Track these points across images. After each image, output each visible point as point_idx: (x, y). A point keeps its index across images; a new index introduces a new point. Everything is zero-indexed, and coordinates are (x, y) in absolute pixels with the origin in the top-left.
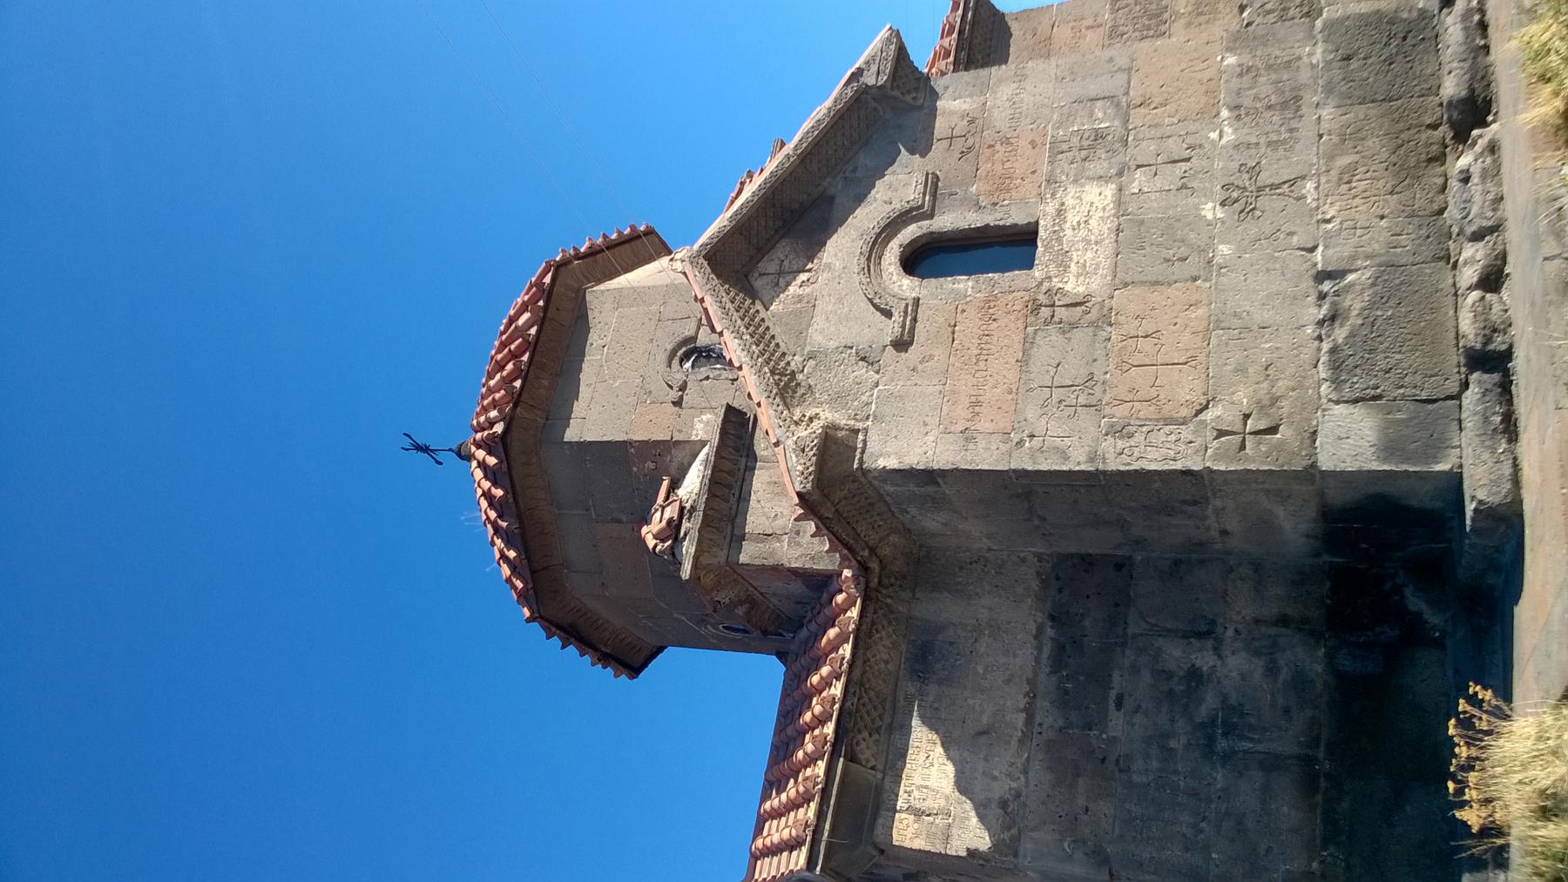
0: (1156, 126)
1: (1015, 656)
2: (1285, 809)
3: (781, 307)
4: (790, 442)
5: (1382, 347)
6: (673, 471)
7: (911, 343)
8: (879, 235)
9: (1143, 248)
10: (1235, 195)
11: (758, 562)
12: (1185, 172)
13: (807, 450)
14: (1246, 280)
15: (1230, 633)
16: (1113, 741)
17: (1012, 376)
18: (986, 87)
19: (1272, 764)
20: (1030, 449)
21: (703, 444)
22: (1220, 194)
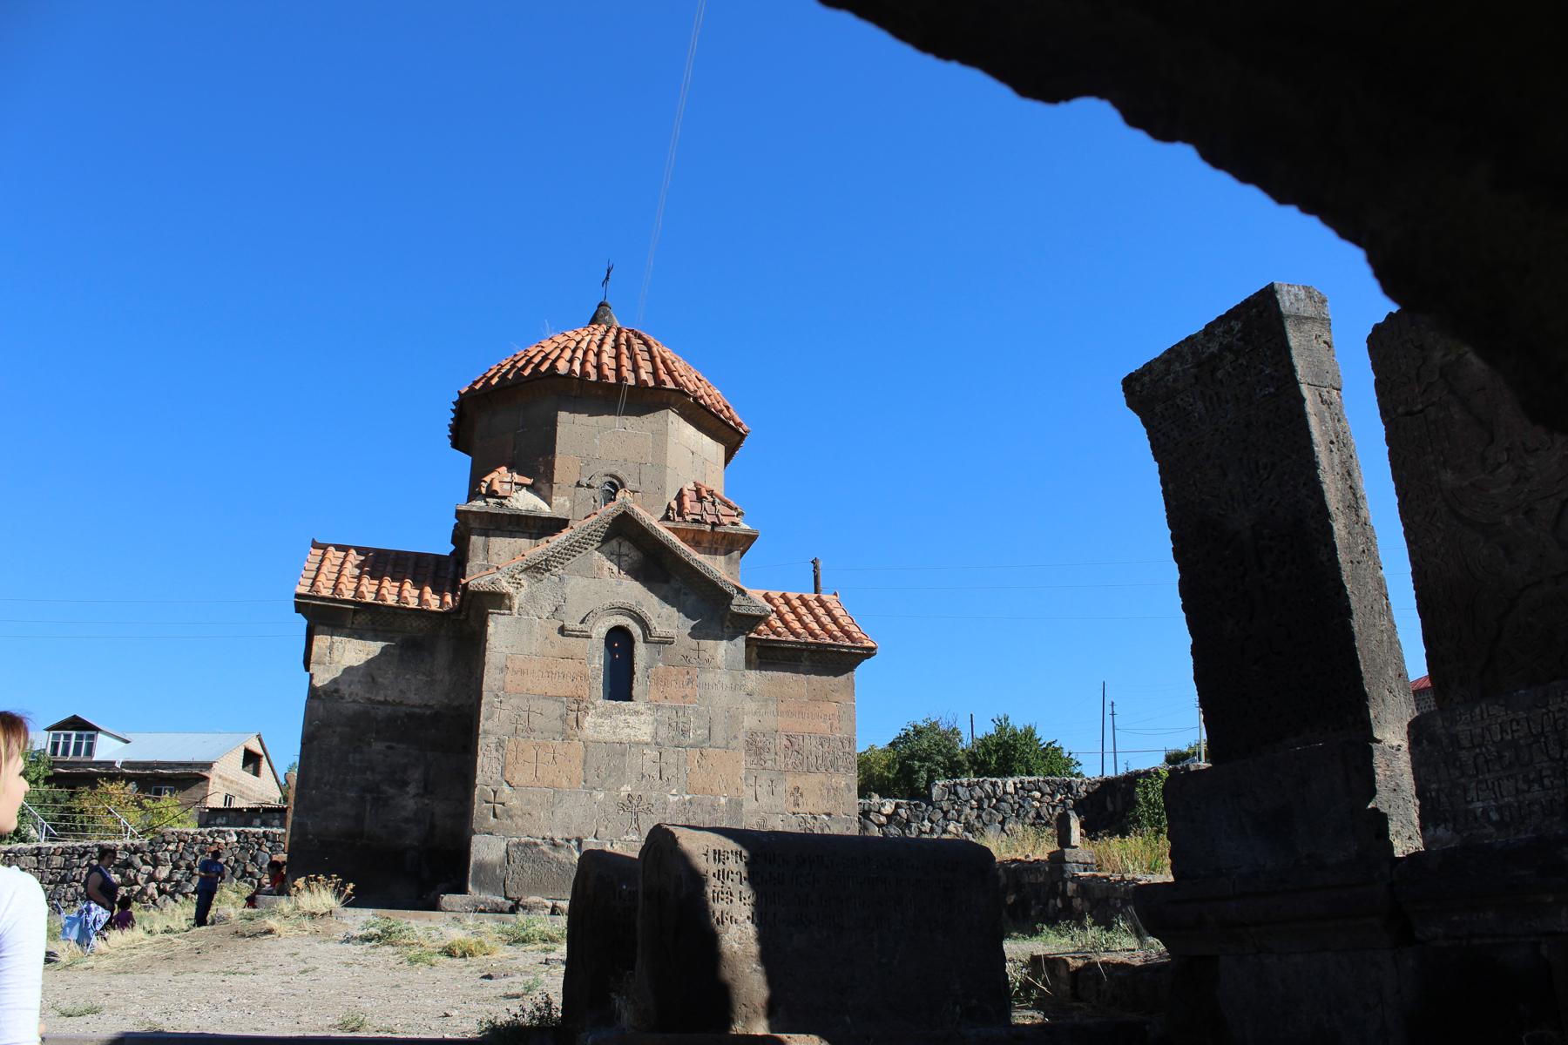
1: (415, 694)
2: (337, 824)
4: (498, 576)
7: (563, 635)
8: (635, 612)
10: (634, 802)
11: (471, 547)
15: (427, 801)
16: (370, 745)
17: (538, 691)
18: (730, 668)
20: (494, 701)
21: (550, 505)
22: (635, 794)
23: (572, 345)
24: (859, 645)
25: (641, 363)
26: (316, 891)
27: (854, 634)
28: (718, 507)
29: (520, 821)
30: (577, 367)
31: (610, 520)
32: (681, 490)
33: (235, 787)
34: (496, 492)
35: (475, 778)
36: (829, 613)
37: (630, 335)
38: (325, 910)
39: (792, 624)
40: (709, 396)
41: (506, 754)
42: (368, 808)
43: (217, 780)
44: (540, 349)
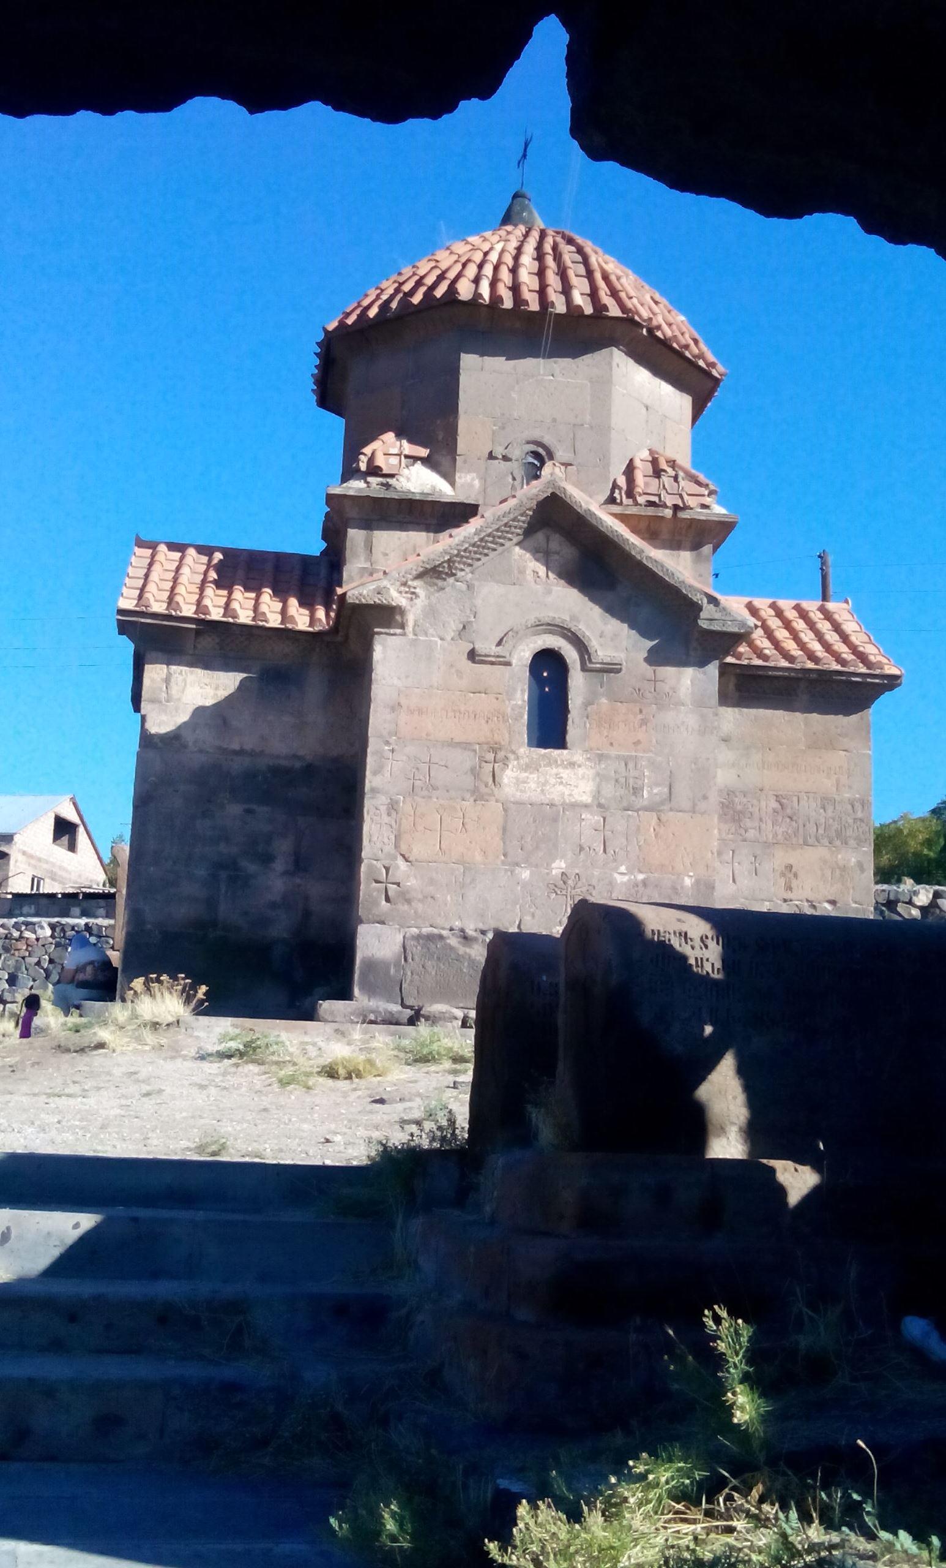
0: (638, 829)
3: (516, 557)
4: (385, 583)
5: (441, 965)
6: (437, 457)
7: (474, 662)
8: (569, 630)
9: (535, 821)
10: (570, 882)
11: (348, 544)
12: (594, 850)
13: (379, 596)
14: (500, 887)
18: (699, 703)
19: (211, 903)
21: (452, 483)
23: (478, 257)
24: (878, 672)
25: (574, 280)
26: (158, 995)
27: (872, 658)
28: (682, 483)
29: (420, 907)
30: (485, 290)
31: (534, 504)
32: (631, 460)
33: (45, 866)
34: (379, 468)
35: (361, 850)
36: (837, 628)
37: (559, 239)
38: (170, 1019)
39: (784, 645)
40: (670, 325)
41: (401, 819)
42: (223, 891)
43: (20, 857)
44: (433, 264)
